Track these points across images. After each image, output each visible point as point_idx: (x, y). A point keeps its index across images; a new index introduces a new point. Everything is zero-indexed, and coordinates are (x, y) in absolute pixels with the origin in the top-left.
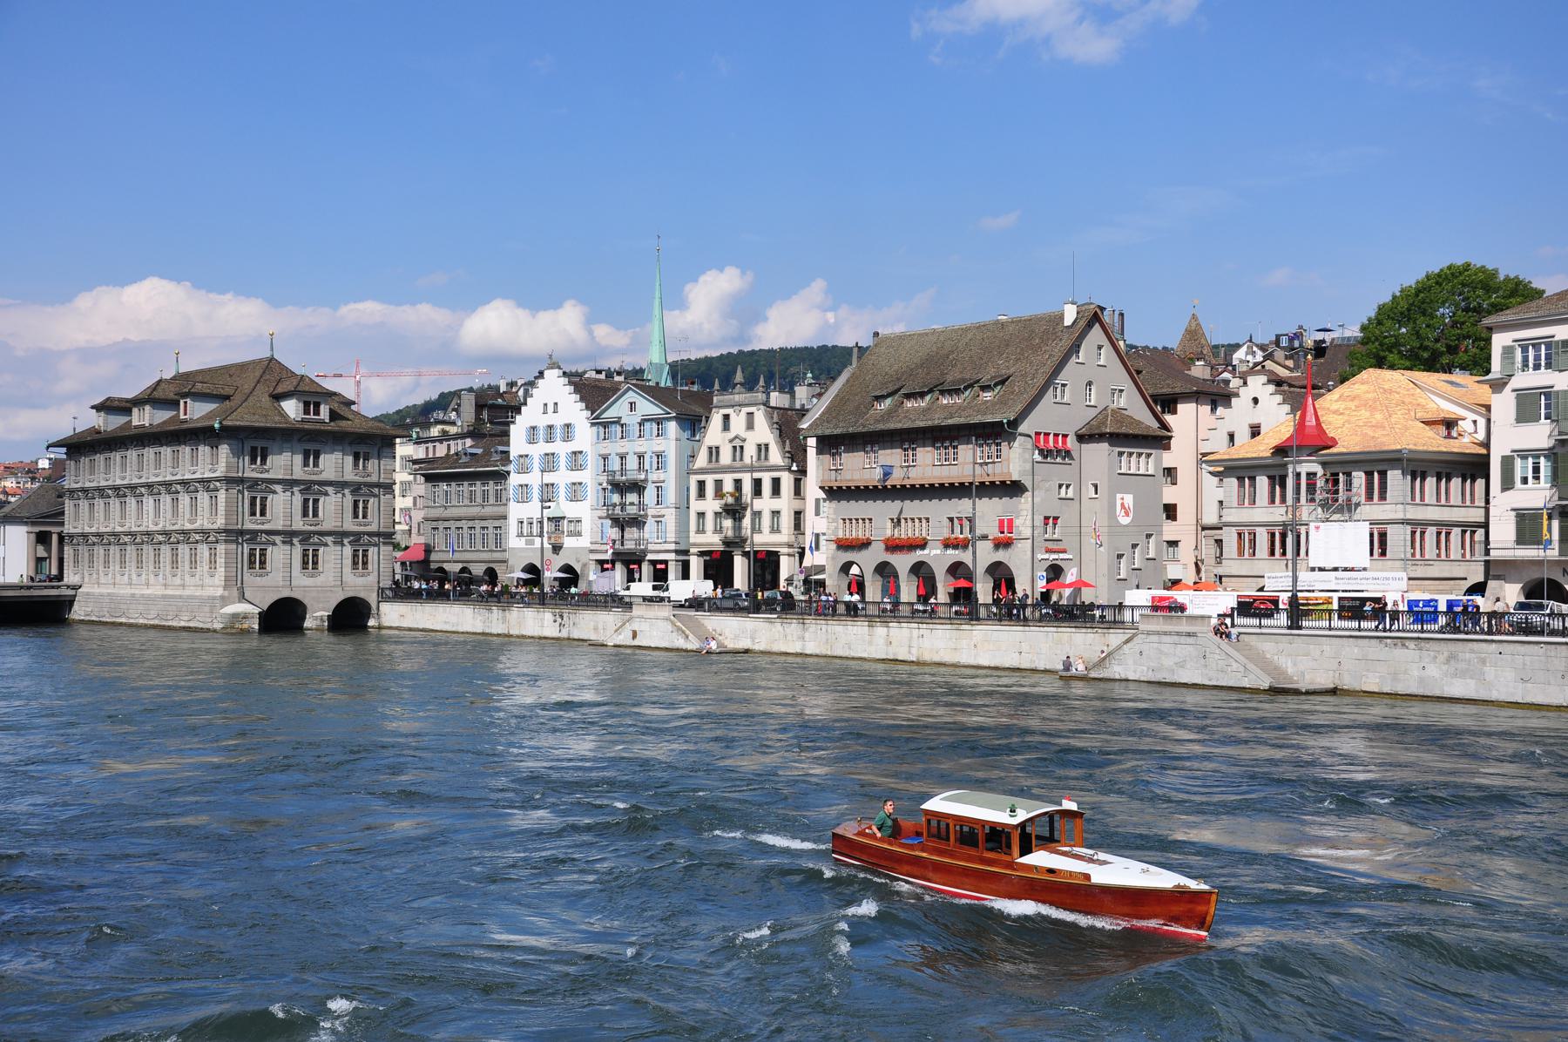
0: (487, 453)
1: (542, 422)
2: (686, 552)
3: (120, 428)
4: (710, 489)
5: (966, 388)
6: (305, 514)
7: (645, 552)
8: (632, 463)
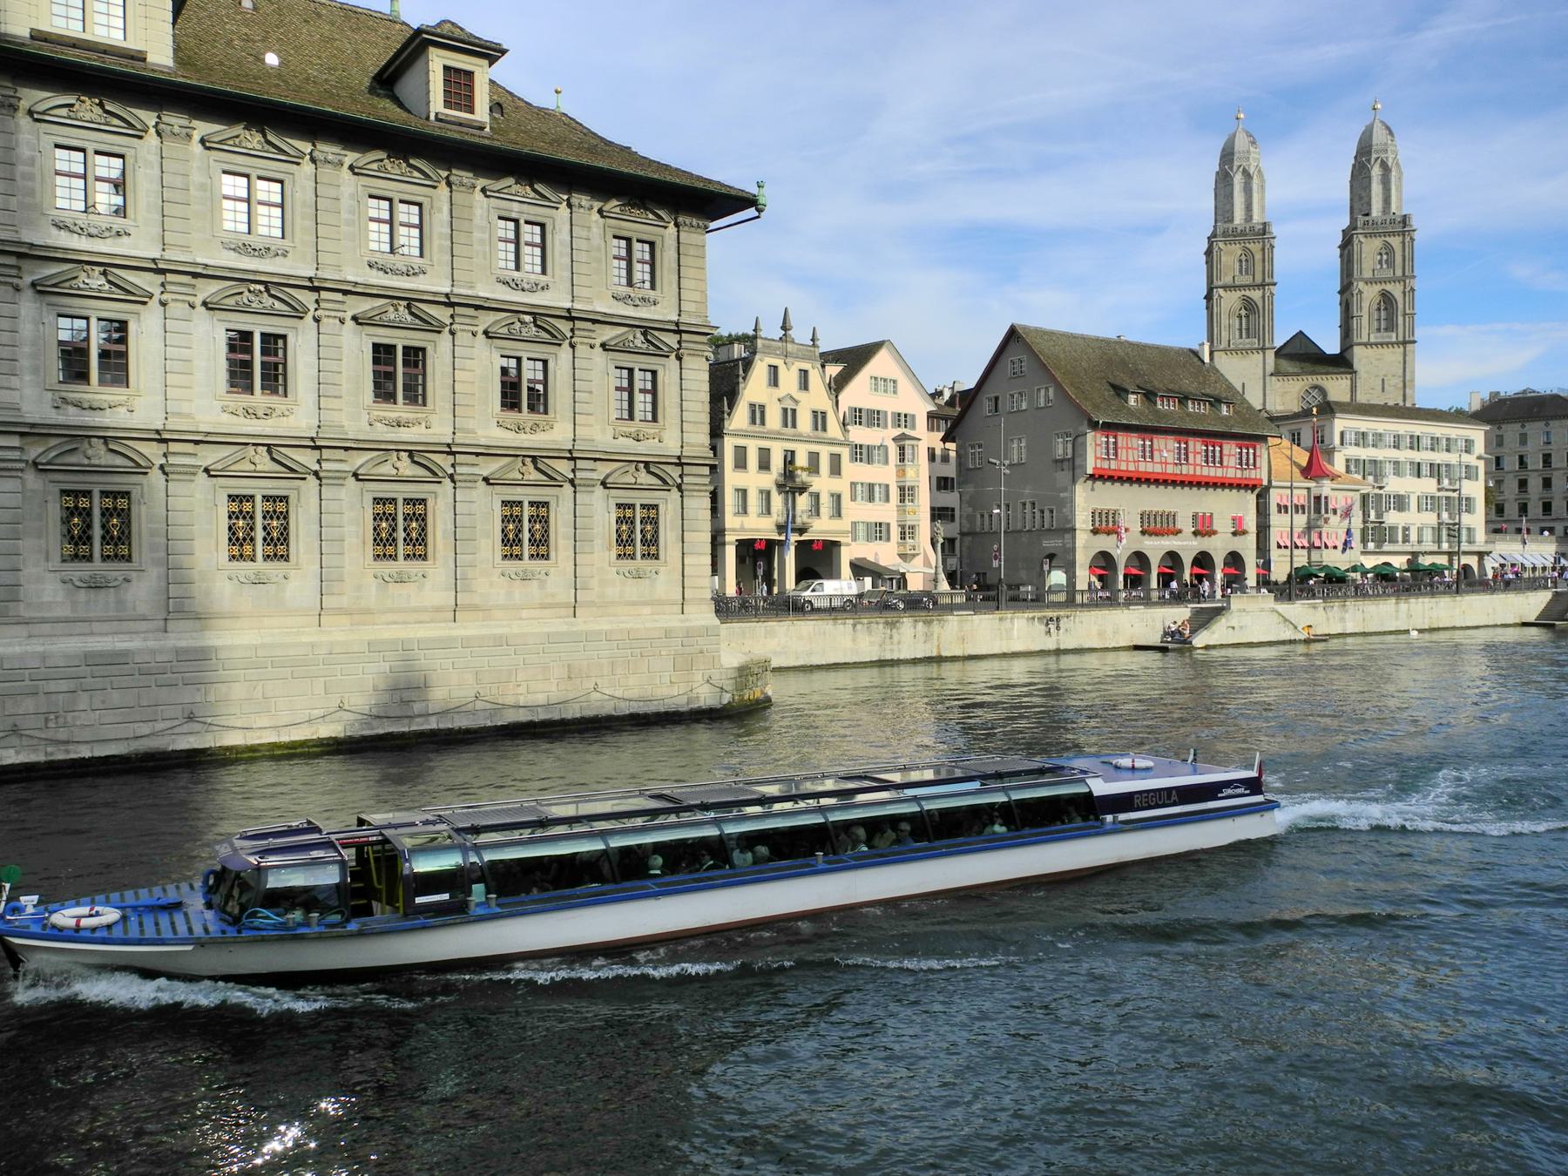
4: (753, 459)
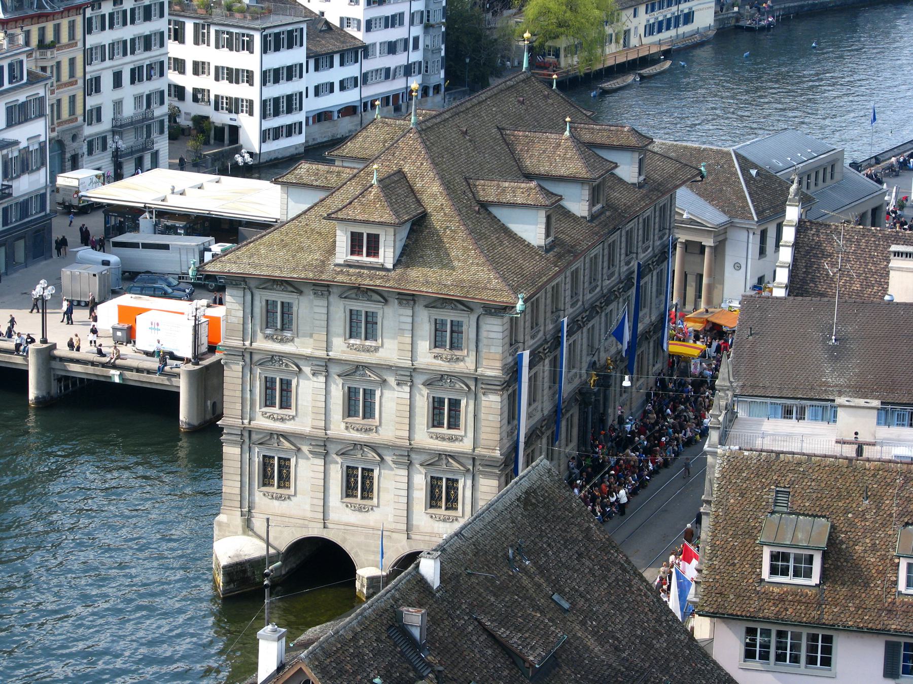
6: (350, 410)
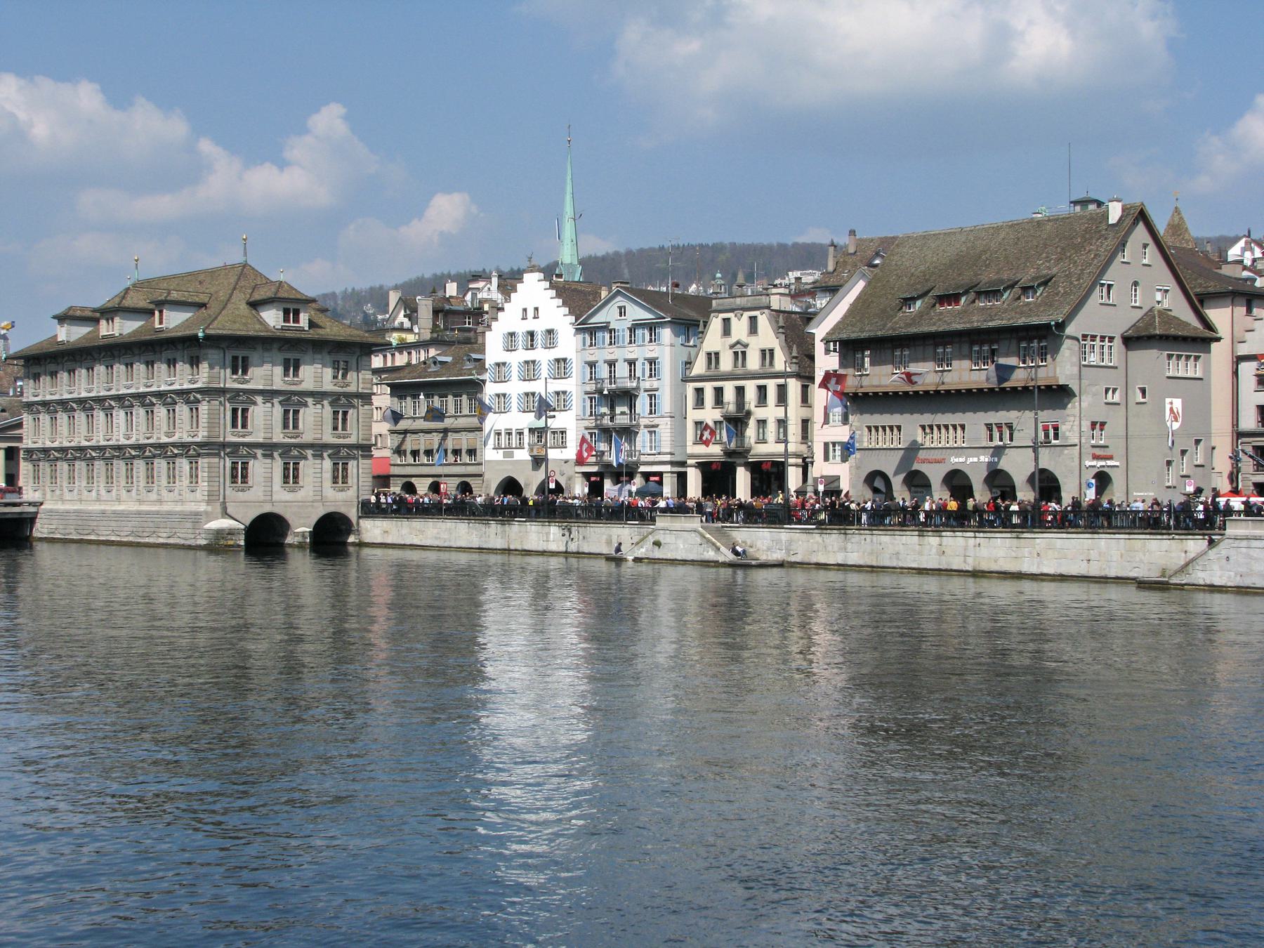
0: (458, 360)
1: (521, 328)
2: (683, 464)
3: (84, 337)
5: (1005, 290)
6: (286, 426)
7: (637, 464)
8: (622, 370)
